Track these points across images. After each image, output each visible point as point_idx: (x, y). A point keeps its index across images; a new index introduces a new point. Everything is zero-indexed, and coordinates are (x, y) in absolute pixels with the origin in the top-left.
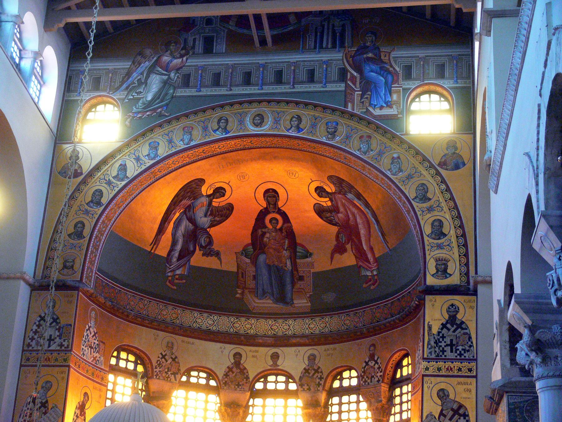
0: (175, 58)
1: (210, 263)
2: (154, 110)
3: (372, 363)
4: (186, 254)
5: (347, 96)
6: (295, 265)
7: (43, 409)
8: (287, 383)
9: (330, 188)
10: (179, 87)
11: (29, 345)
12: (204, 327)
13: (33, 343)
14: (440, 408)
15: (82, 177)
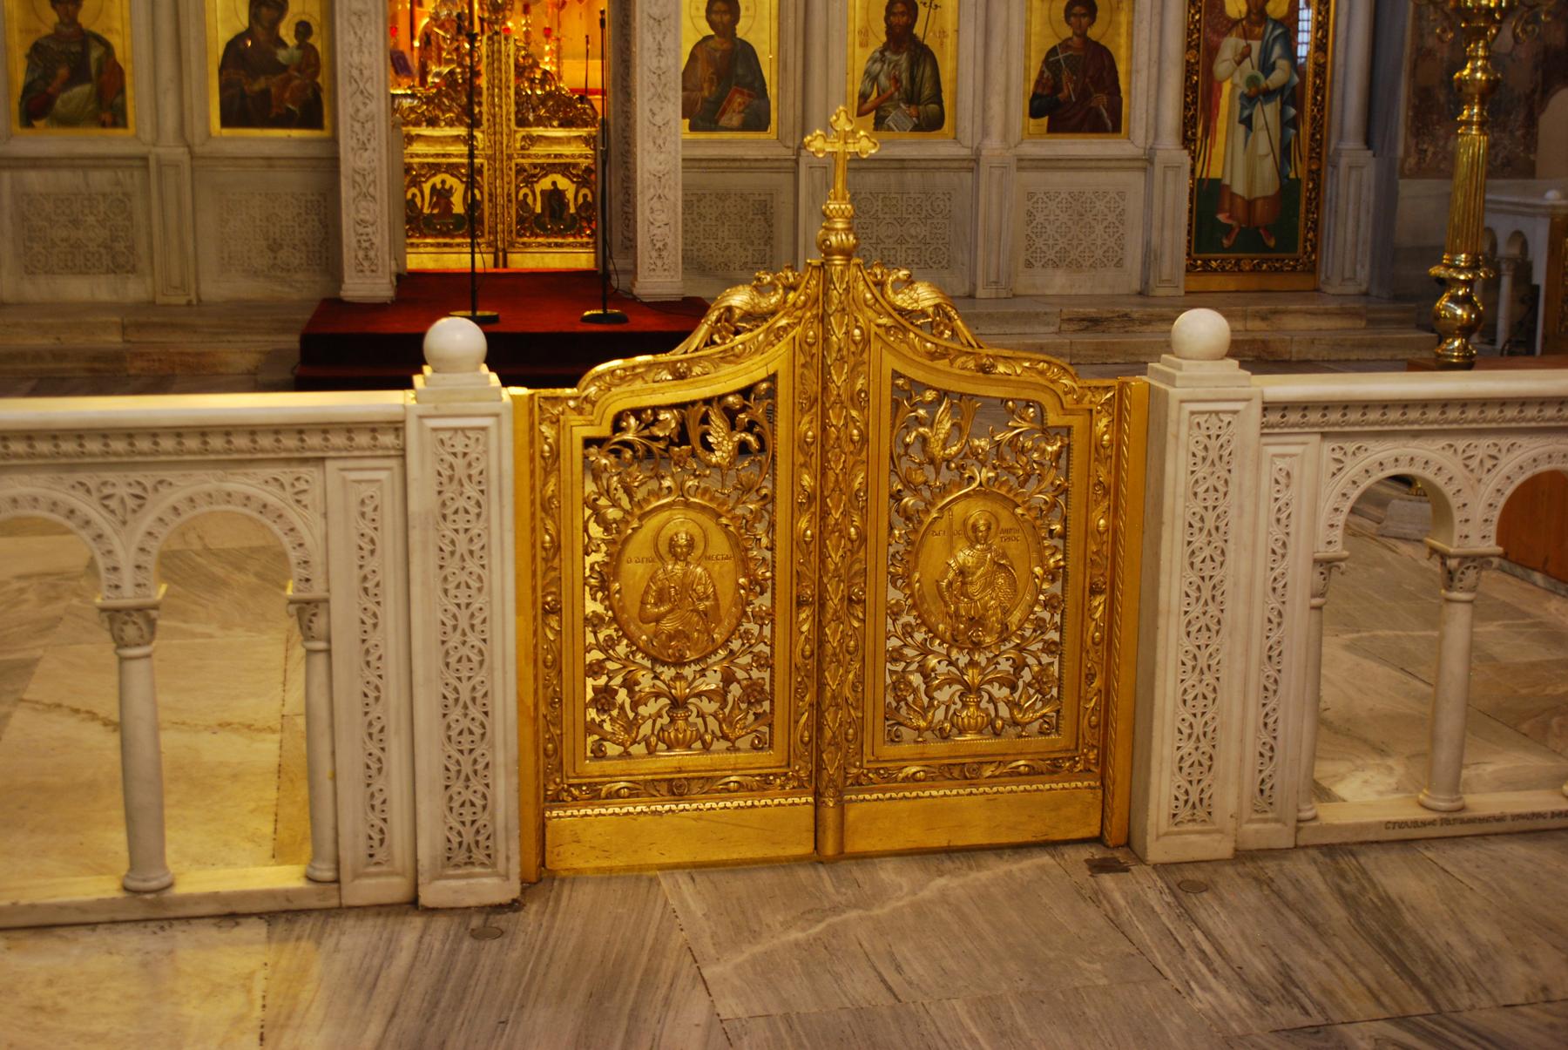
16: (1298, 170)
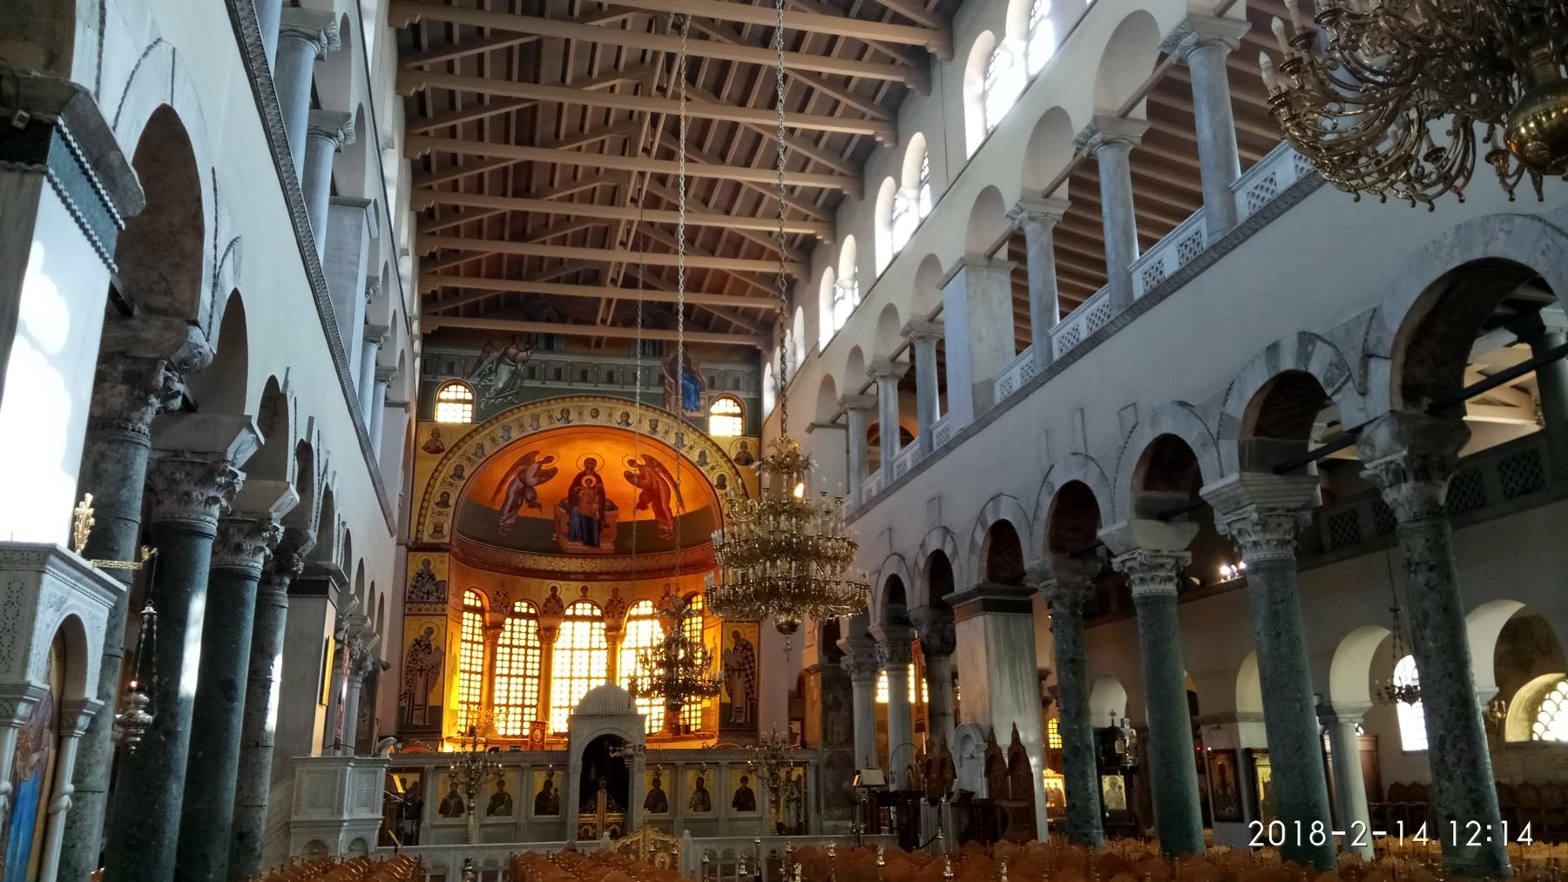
0: (520, 350)
1: (534, 513)
2: (506, 397)
3: (667, 599)
4: (515, 506)
5: (664, 399)
6: (602, 516)
7: (427, 650)
8: (592, 609)
9: (642, 462)
10: (525, 379)
11: (410, 598)
12: (527, 567)
13: (414, 596)
14: (734, 645)
15: (444, 454)
16: (802, 820)
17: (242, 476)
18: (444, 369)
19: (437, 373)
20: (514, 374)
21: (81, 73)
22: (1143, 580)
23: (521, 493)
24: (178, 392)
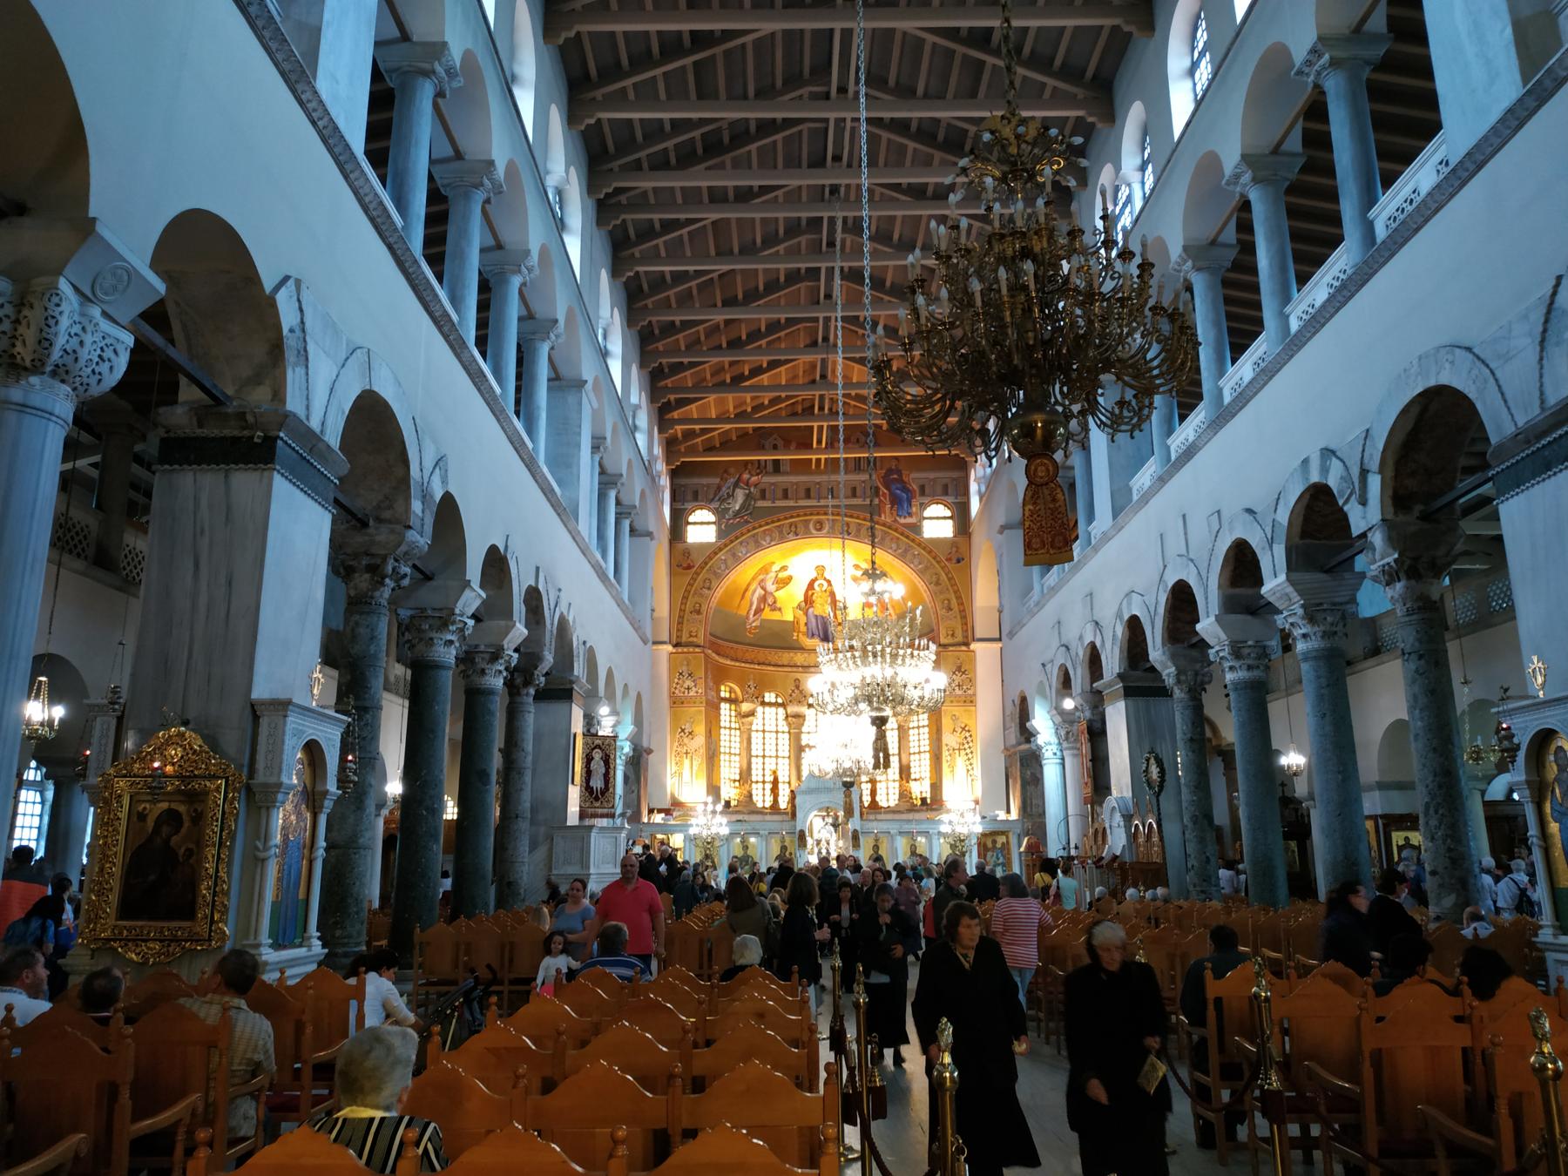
1: (775, 616)
4: (759, 611)
17: (471, 623)
18: (689, 496)
19: (684, 501)
20: (748, 497)
21: (294, 404)
22: (1231, 668)
23: (763, 599)
24: (406, 575)
